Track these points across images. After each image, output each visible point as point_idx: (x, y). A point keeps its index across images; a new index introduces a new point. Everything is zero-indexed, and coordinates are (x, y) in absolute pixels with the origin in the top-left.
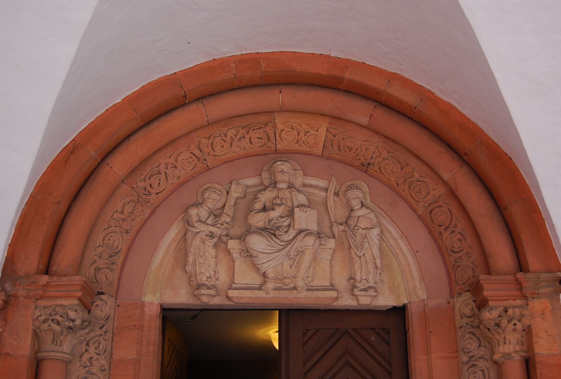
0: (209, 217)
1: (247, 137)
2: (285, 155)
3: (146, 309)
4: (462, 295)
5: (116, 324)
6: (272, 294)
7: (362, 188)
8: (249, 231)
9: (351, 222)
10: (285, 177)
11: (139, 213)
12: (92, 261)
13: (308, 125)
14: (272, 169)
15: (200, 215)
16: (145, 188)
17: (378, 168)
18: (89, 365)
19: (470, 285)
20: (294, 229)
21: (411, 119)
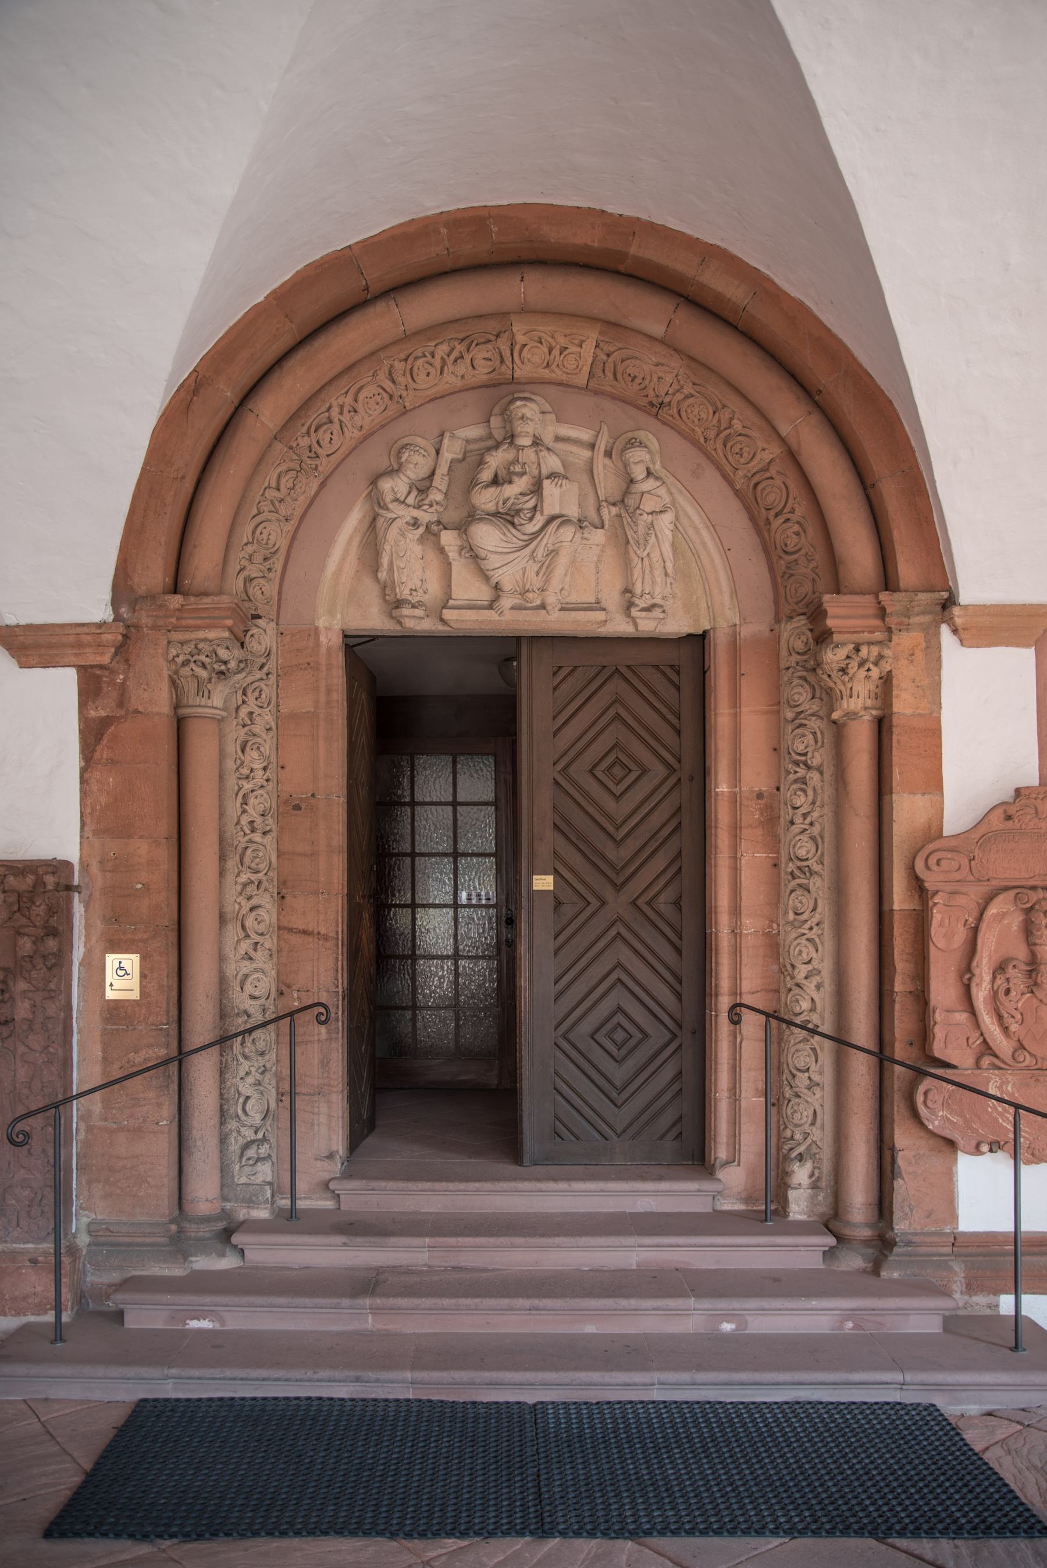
0: (409, 493)
1: (468, 358)
2: (526, 386)
3: (323, 639)
4: (794, 620)
5: (280, 661)
6: (509, 616)
7: (648, 443)
8: (472, 517)
9: (630, 501)
10: (530, 428)
11: (303, 488)
12: (238, 568)
13: (565, 336)
14: (508, 412)
15: (396, 490)
16: (310, 446)
17: (675, 411)
18: (249, 723)
19: (807, 605)
20: (542, 514)
21: (735, 327)
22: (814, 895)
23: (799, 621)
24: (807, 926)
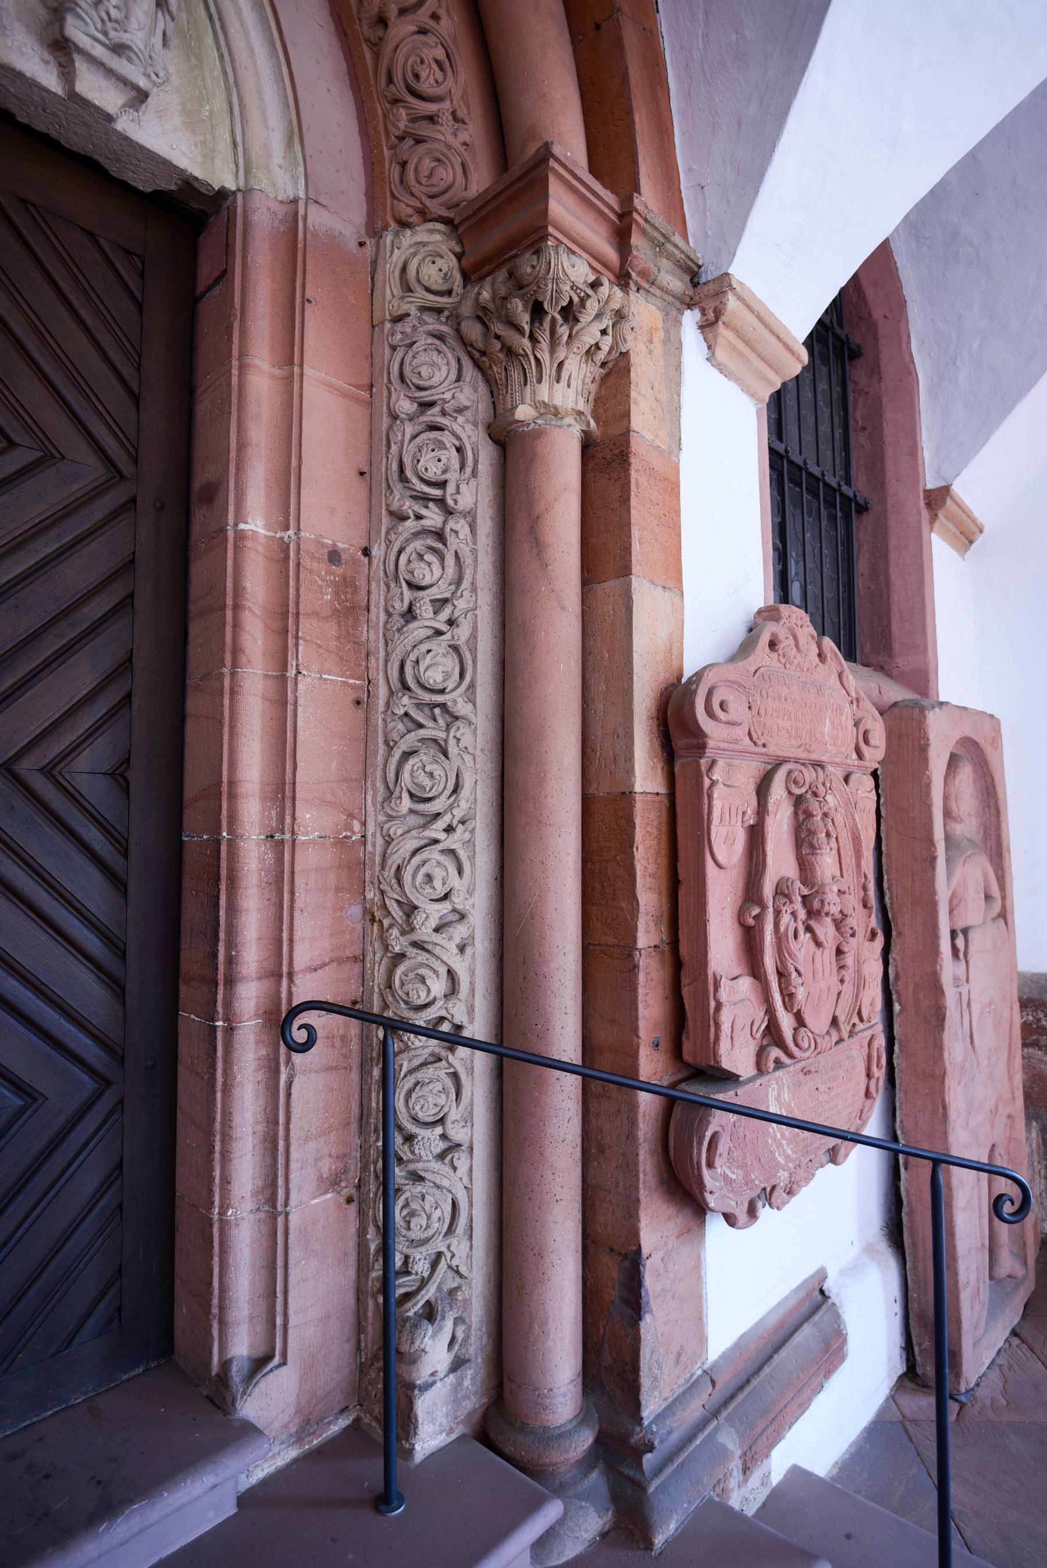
22: (456, 762)
23: (431, 231)
24: (441, 824)
